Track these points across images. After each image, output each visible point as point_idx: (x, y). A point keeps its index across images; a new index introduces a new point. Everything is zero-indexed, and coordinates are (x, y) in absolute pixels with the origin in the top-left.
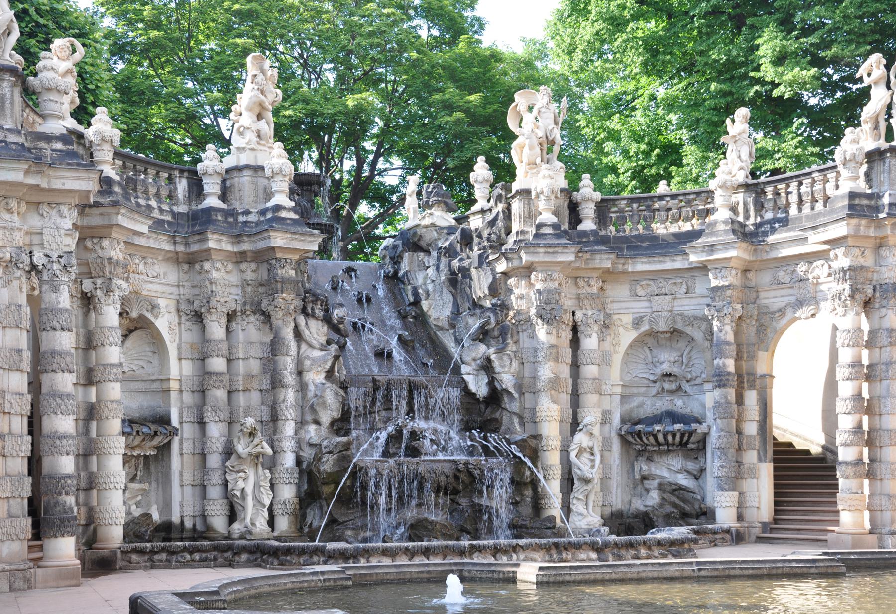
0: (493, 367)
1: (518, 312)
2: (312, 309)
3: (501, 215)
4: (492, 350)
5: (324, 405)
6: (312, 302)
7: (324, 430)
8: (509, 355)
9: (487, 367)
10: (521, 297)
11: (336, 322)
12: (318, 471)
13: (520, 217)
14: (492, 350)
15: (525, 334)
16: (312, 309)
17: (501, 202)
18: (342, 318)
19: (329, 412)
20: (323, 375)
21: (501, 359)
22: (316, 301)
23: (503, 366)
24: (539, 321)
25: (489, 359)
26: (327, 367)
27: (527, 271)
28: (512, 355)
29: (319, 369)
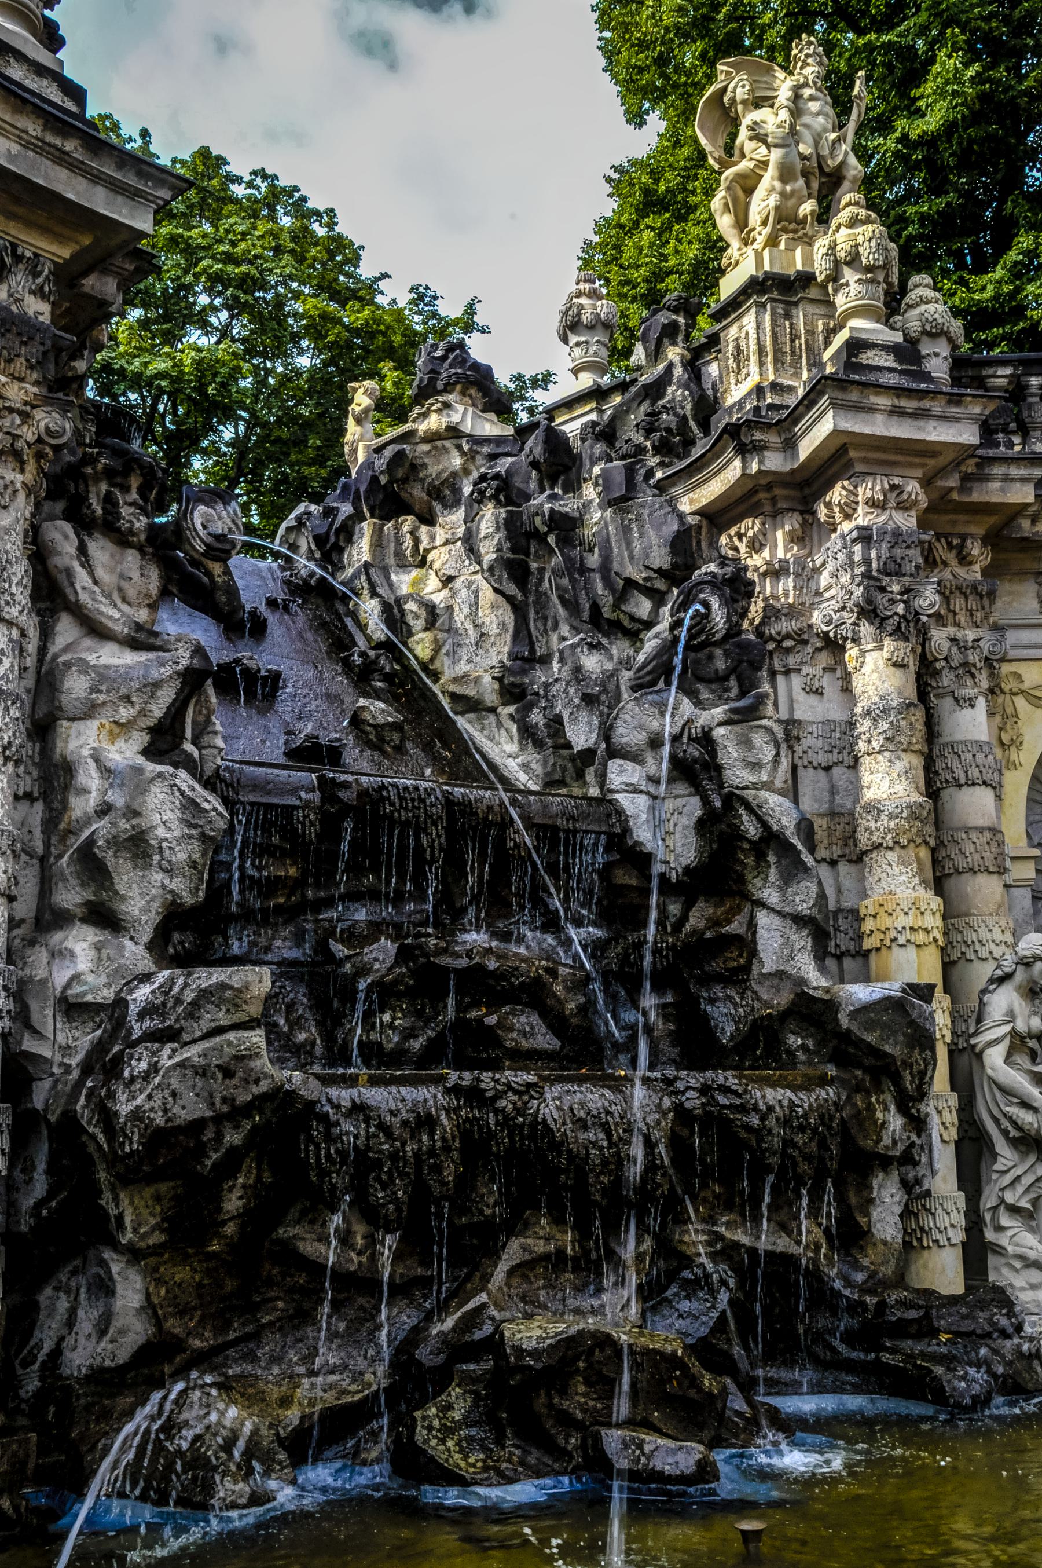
0: (719, 769)
1: (771, 613)
2: (109, 501)
3: (678, 371)
4: (719, 712)
5: (138, 846)
6: (109, 474)
7: (134, 953)
8: (768, 730)
9: (694, 765)
10: (776, 572)
11: (201, 548)
12: (107, 1117)
13: (761, 351)
14: (719, 712)
15: (796, 681)
16: (109, 501)
17: (674, 343)
18: (220, 538)
19: (158, 877)
20: (140, 739)
21: (746, 743)
22: (126, 472)
23: (755, 766)
24: (866, 629)
25: (706, 739)
26: (158, 709)
27: (798, 494)
28: (779, 730)
29: (125, 713)
